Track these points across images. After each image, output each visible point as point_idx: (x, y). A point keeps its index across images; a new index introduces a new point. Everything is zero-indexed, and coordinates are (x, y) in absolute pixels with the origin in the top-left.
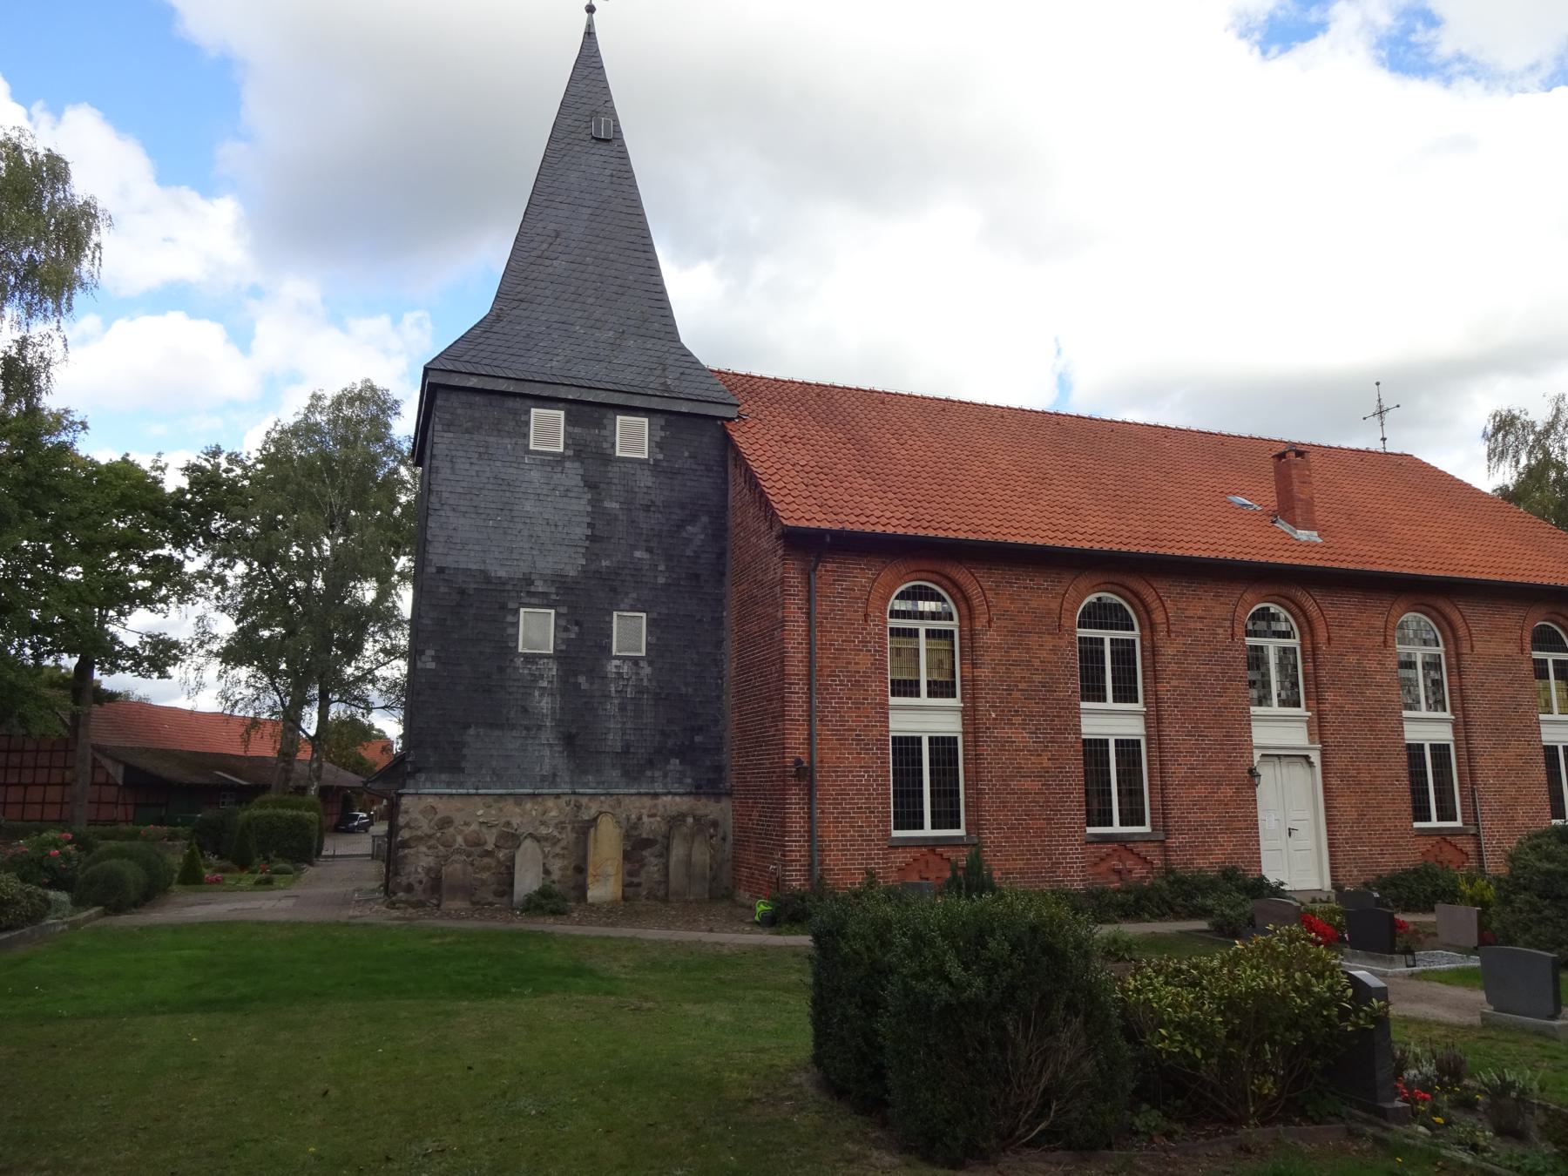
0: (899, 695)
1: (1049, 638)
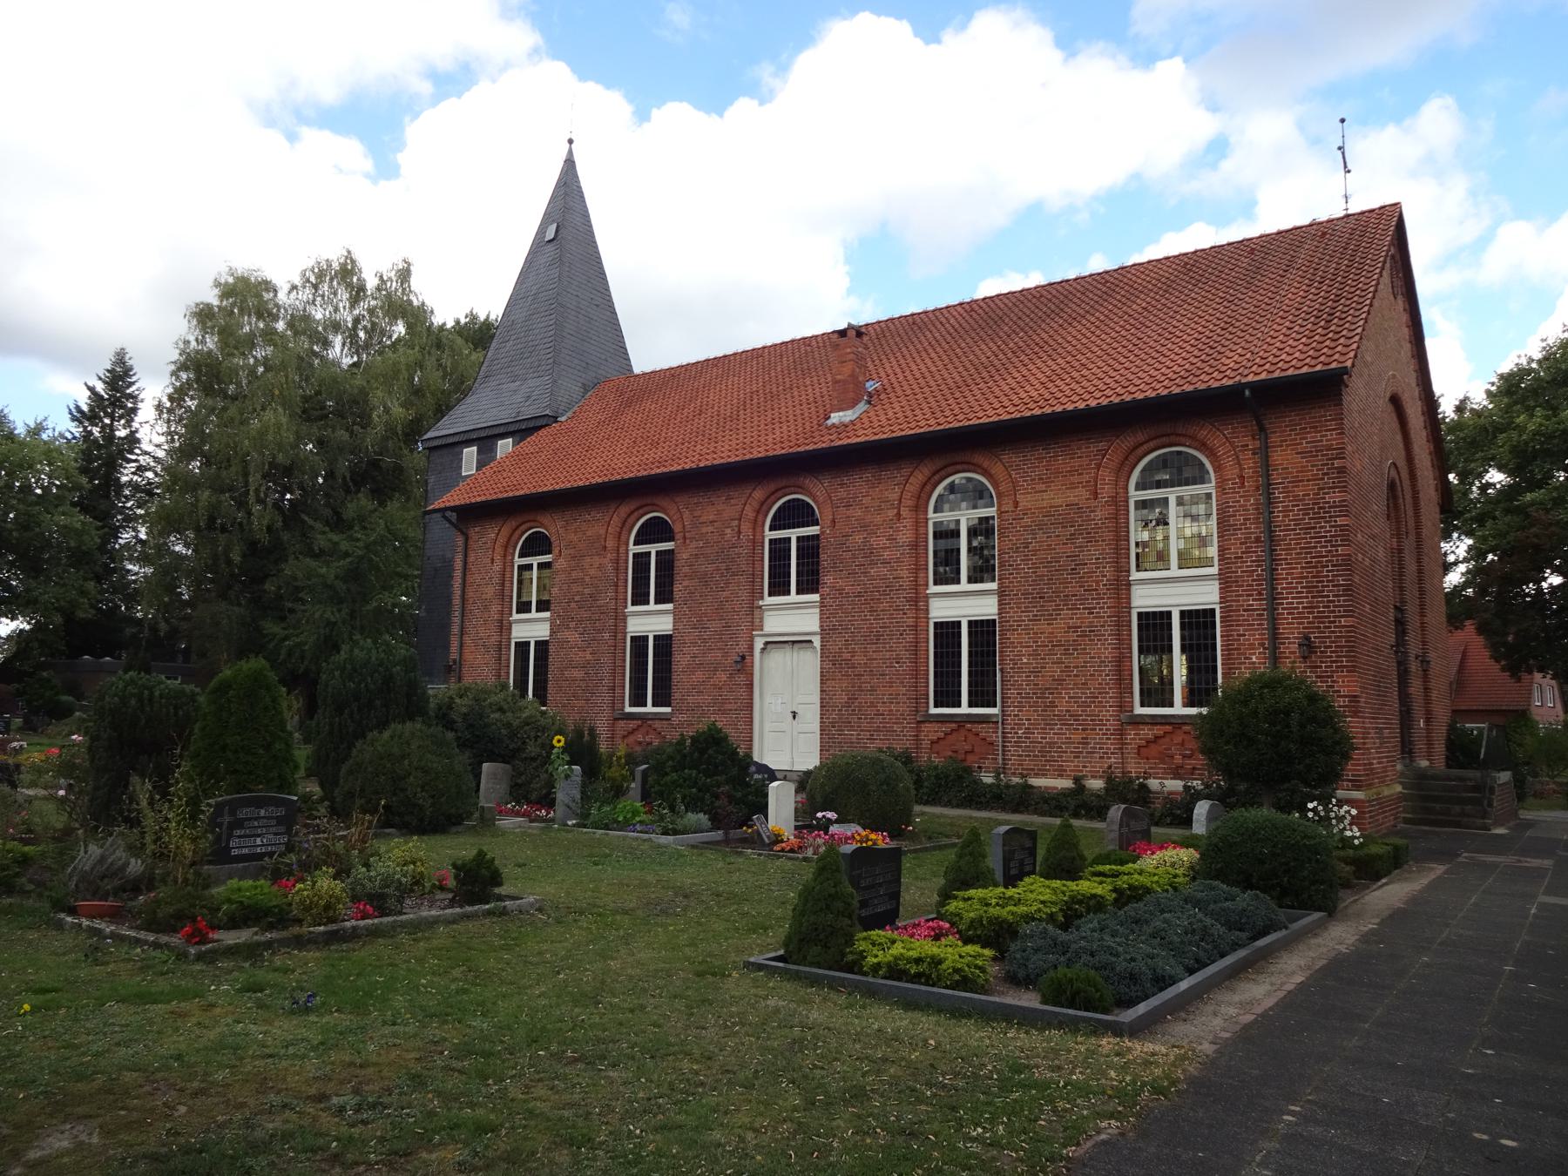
0: (941, 584)
1: (596, 558)
